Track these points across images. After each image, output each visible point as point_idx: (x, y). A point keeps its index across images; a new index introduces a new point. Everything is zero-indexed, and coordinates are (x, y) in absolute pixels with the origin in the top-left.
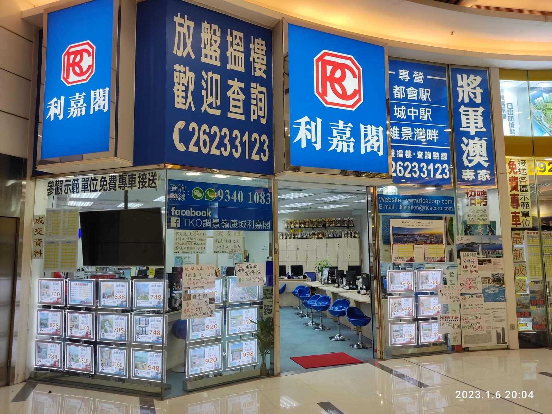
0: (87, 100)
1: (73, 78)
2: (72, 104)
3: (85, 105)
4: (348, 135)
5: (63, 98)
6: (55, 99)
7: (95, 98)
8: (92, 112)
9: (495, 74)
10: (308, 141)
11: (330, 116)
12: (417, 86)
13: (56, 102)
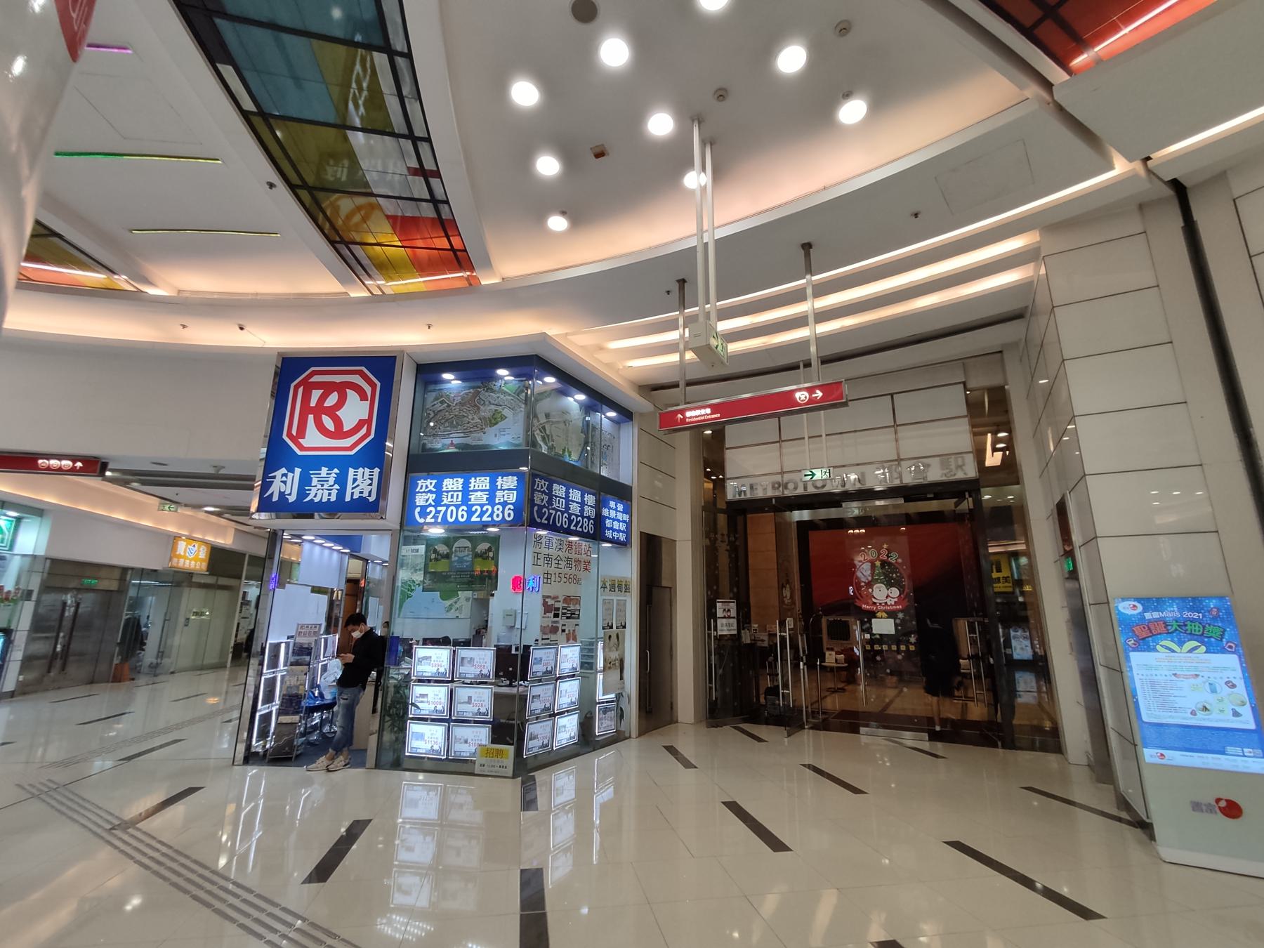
4: (331, 482)
10: (282, 494)
11: (311, 464)
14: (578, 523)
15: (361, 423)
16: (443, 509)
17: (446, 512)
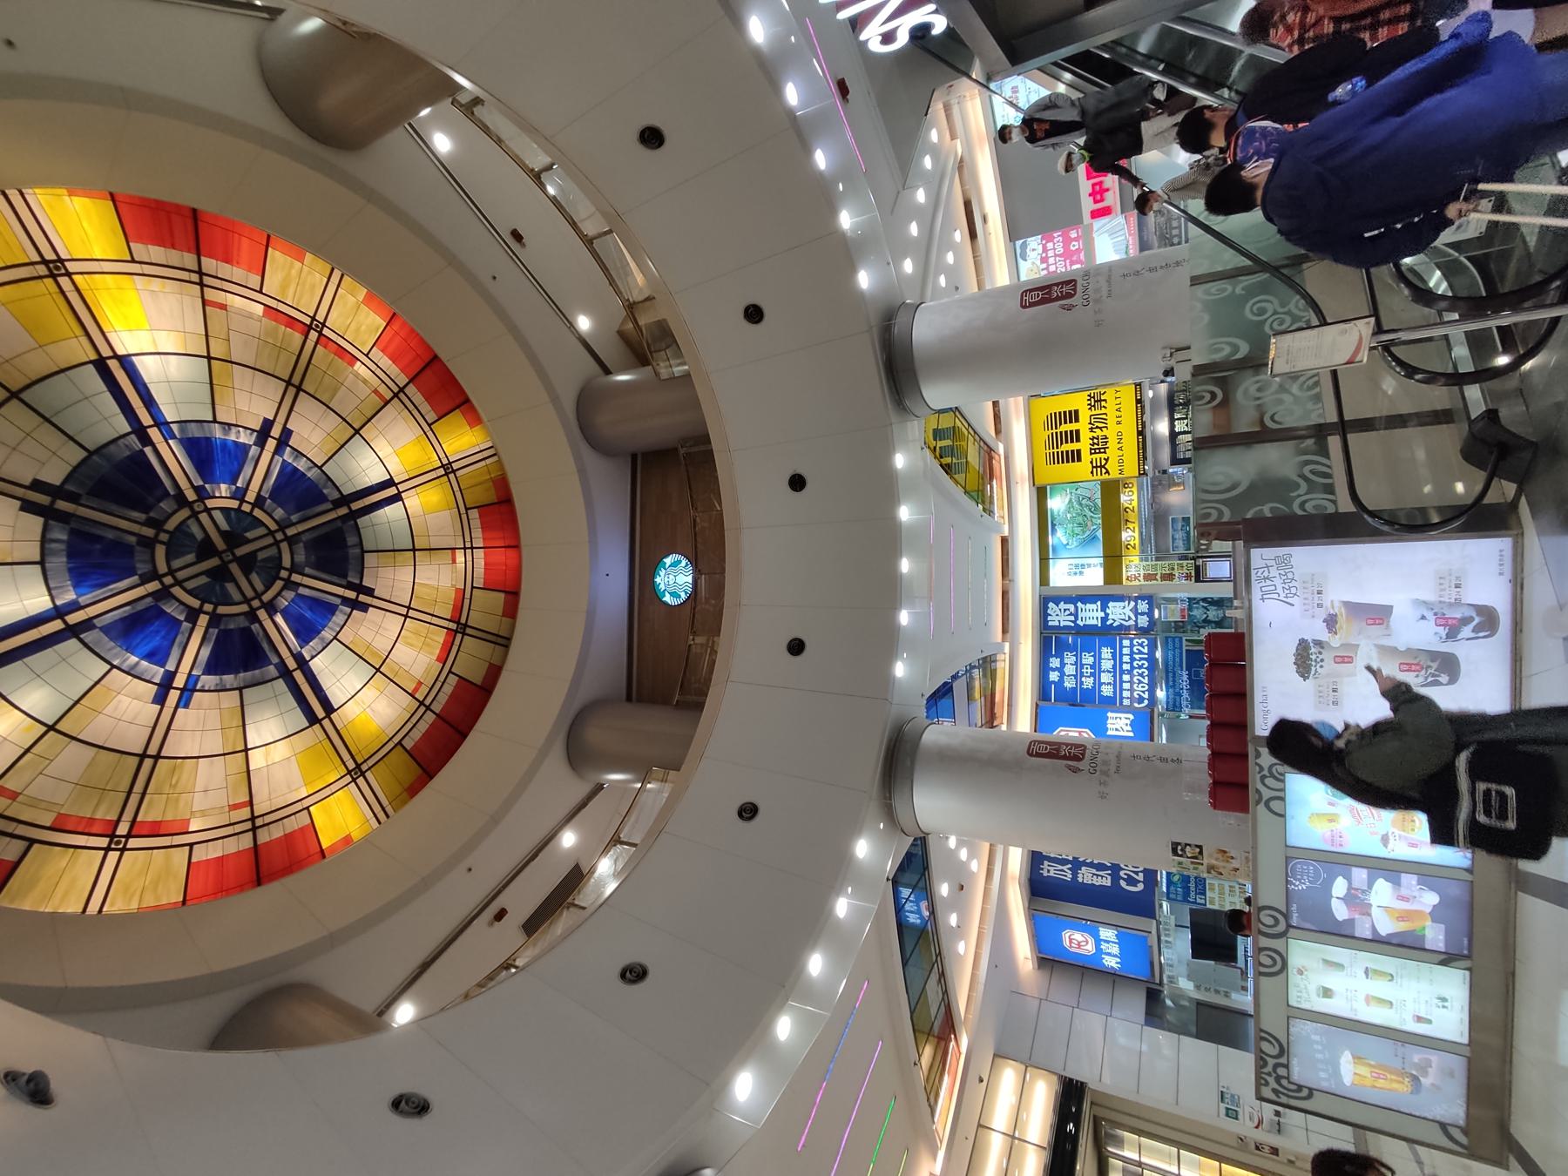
9: (1047, 592)
12: (1063, 664)
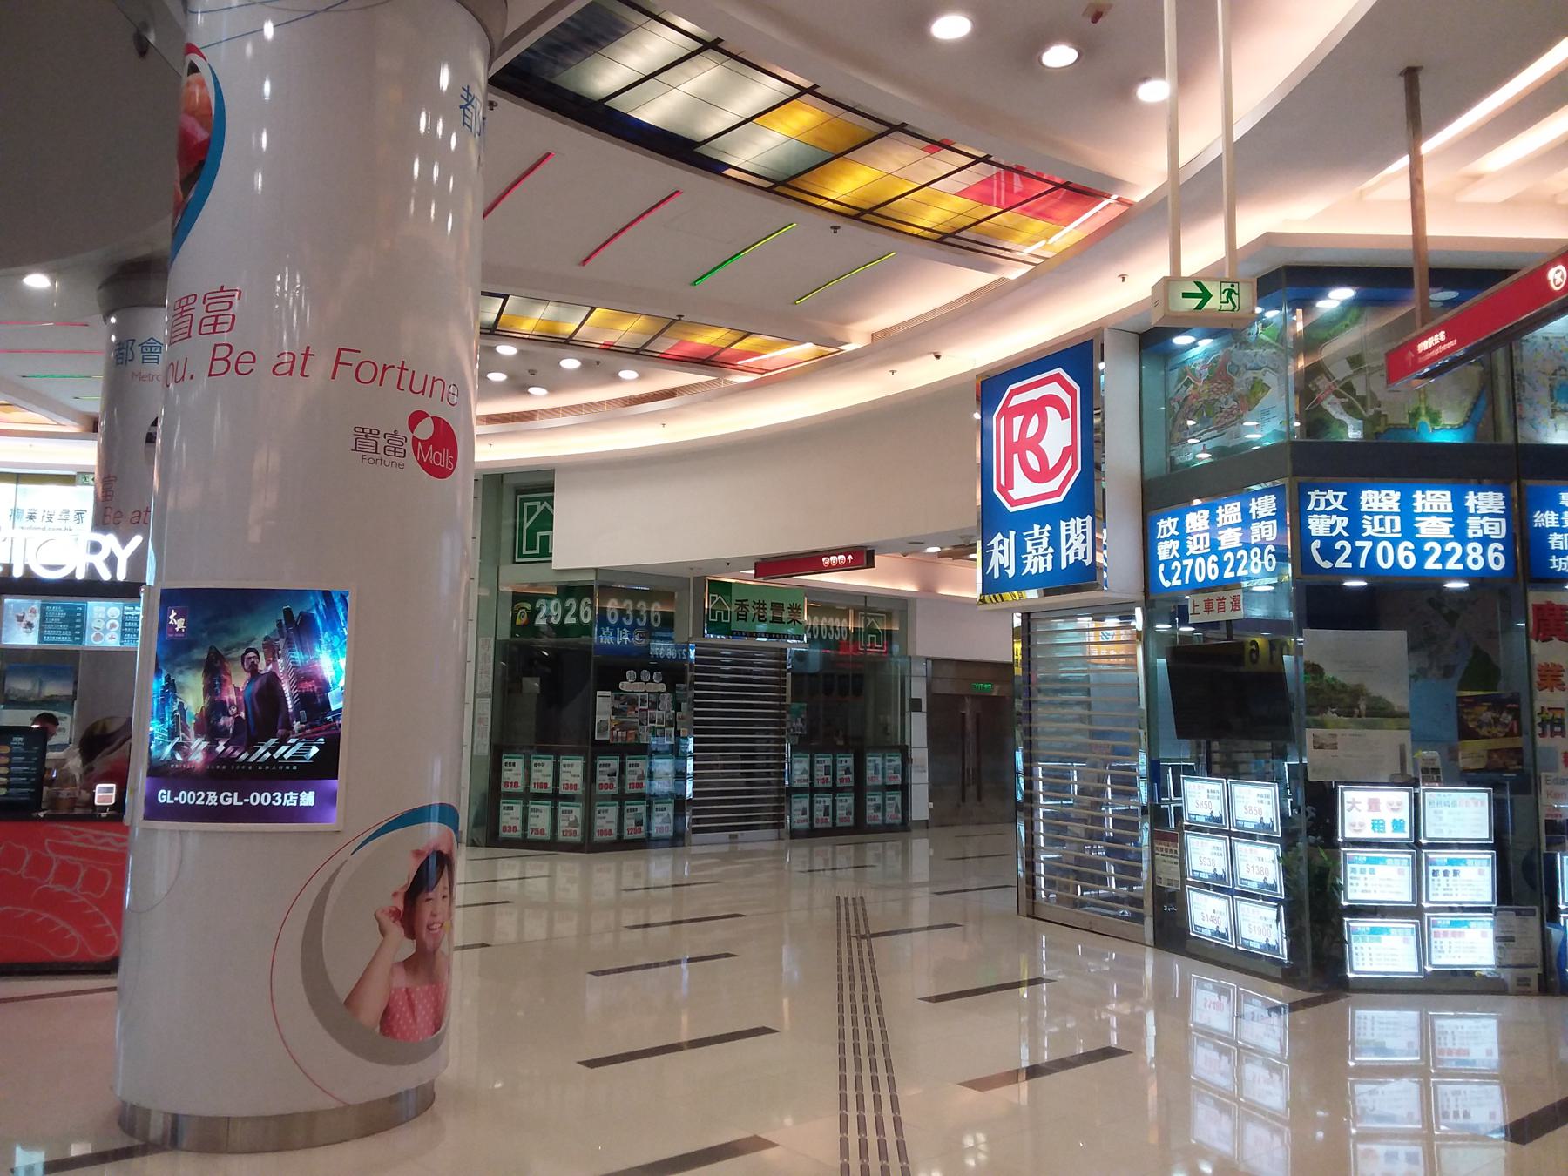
0: (1054, 541)
1: (1023, 487)
2: (1029, 547)
3: (1051, 550)
5: (1012, 534)
6: (999, 536)
7: (1068, 537)
8: (1064, 566)
13: (1001, 542)
14: (1237, 562)
15: (1067, 452)
16: (1189, 562)
17: (1372, 552)
